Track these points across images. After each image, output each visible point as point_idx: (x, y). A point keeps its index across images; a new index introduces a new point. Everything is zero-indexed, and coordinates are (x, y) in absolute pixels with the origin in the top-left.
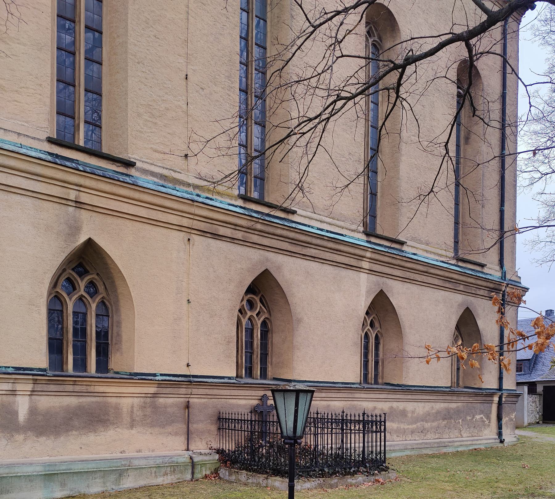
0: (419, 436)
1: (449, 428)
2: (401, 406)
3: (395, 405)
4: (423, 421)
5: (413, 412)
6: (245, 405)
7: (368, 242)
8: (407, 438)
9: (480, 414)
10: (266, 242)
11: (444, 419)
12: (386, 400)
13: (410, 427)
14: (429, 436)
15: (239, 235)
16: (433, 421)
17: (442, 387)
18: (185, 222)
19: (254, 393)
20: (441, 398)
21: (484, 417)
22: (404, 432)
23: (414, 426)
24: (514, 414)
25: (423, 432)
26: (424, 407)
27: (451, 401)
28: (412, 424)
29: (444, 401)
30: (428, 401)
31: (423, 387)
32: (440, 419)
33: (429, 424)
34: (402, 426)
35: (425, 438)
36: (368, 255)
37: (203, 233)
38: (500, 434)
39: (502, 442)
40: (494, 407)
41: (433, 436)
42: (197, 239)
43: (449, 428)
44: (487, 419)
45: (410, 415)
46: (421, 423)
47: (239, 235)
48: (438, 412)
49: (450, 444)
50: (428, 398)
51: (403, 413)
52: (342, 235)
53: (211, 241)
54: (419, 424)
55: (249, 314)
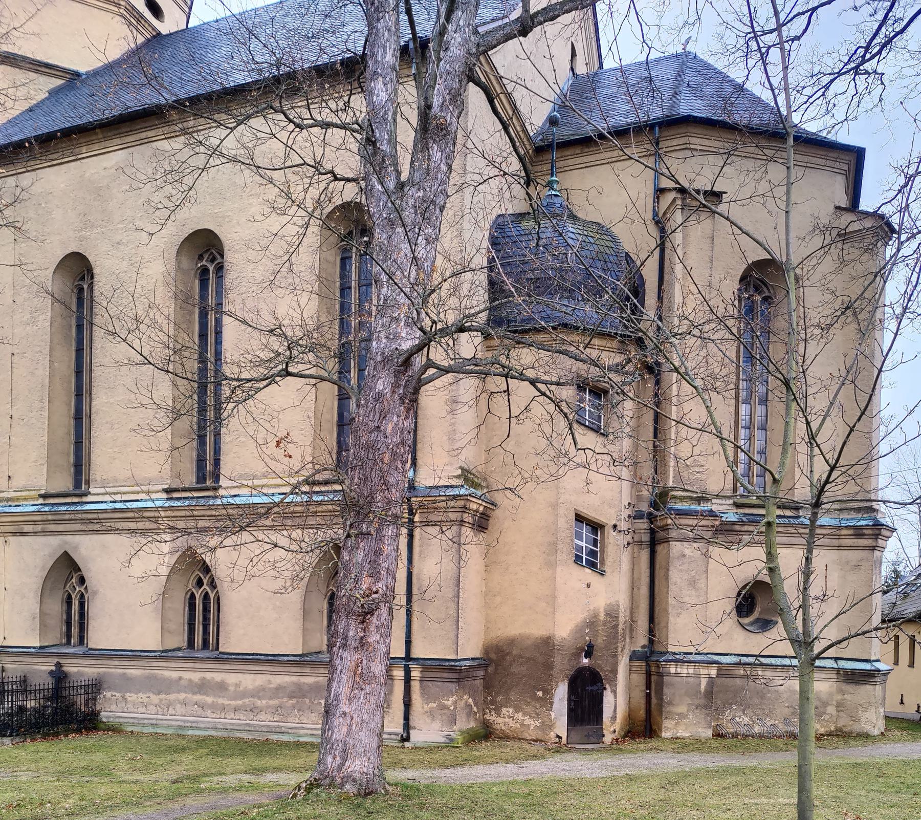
0: (244, 715)
1: (299, 710)
2: (218, 677)
3: (208, 675)
4: (253, 696)
5: (237, 685)
6: (45, 671)
7: (168, 499)
8: (227, 717)
10: (61, 528)
11: (291, 697)
12: (194, 670)
13: (233, 703)
14: (262, 716)
15: (39, 528)
16: (271, 699)
17: (288, 655)
20: (281, 669)
22: (223, 708)
23: (240, 702)
24: (451, 699)
25: (254, 710)
26: (254, 680)
27: (302, 675)
28: (235, 699)
29: (288, 673)
31: (252, 655)
32: (283, 697)
33: (264, 702)
34: (220, 701)
35: (255, 719)
36: (163, 514)
37: (14, 534)
38: (407, 726)
41: (270, 718)
42: (11, 539)
43: (299, 710)
45: (232, 688)
46: (251, 699)
47: (39, 528)
48: (279, 688)
49: (290, 731)
50: (257, 669)
51: (222, 687)
52: (137, 501)
53: (21, 538)
54: (246, 701)
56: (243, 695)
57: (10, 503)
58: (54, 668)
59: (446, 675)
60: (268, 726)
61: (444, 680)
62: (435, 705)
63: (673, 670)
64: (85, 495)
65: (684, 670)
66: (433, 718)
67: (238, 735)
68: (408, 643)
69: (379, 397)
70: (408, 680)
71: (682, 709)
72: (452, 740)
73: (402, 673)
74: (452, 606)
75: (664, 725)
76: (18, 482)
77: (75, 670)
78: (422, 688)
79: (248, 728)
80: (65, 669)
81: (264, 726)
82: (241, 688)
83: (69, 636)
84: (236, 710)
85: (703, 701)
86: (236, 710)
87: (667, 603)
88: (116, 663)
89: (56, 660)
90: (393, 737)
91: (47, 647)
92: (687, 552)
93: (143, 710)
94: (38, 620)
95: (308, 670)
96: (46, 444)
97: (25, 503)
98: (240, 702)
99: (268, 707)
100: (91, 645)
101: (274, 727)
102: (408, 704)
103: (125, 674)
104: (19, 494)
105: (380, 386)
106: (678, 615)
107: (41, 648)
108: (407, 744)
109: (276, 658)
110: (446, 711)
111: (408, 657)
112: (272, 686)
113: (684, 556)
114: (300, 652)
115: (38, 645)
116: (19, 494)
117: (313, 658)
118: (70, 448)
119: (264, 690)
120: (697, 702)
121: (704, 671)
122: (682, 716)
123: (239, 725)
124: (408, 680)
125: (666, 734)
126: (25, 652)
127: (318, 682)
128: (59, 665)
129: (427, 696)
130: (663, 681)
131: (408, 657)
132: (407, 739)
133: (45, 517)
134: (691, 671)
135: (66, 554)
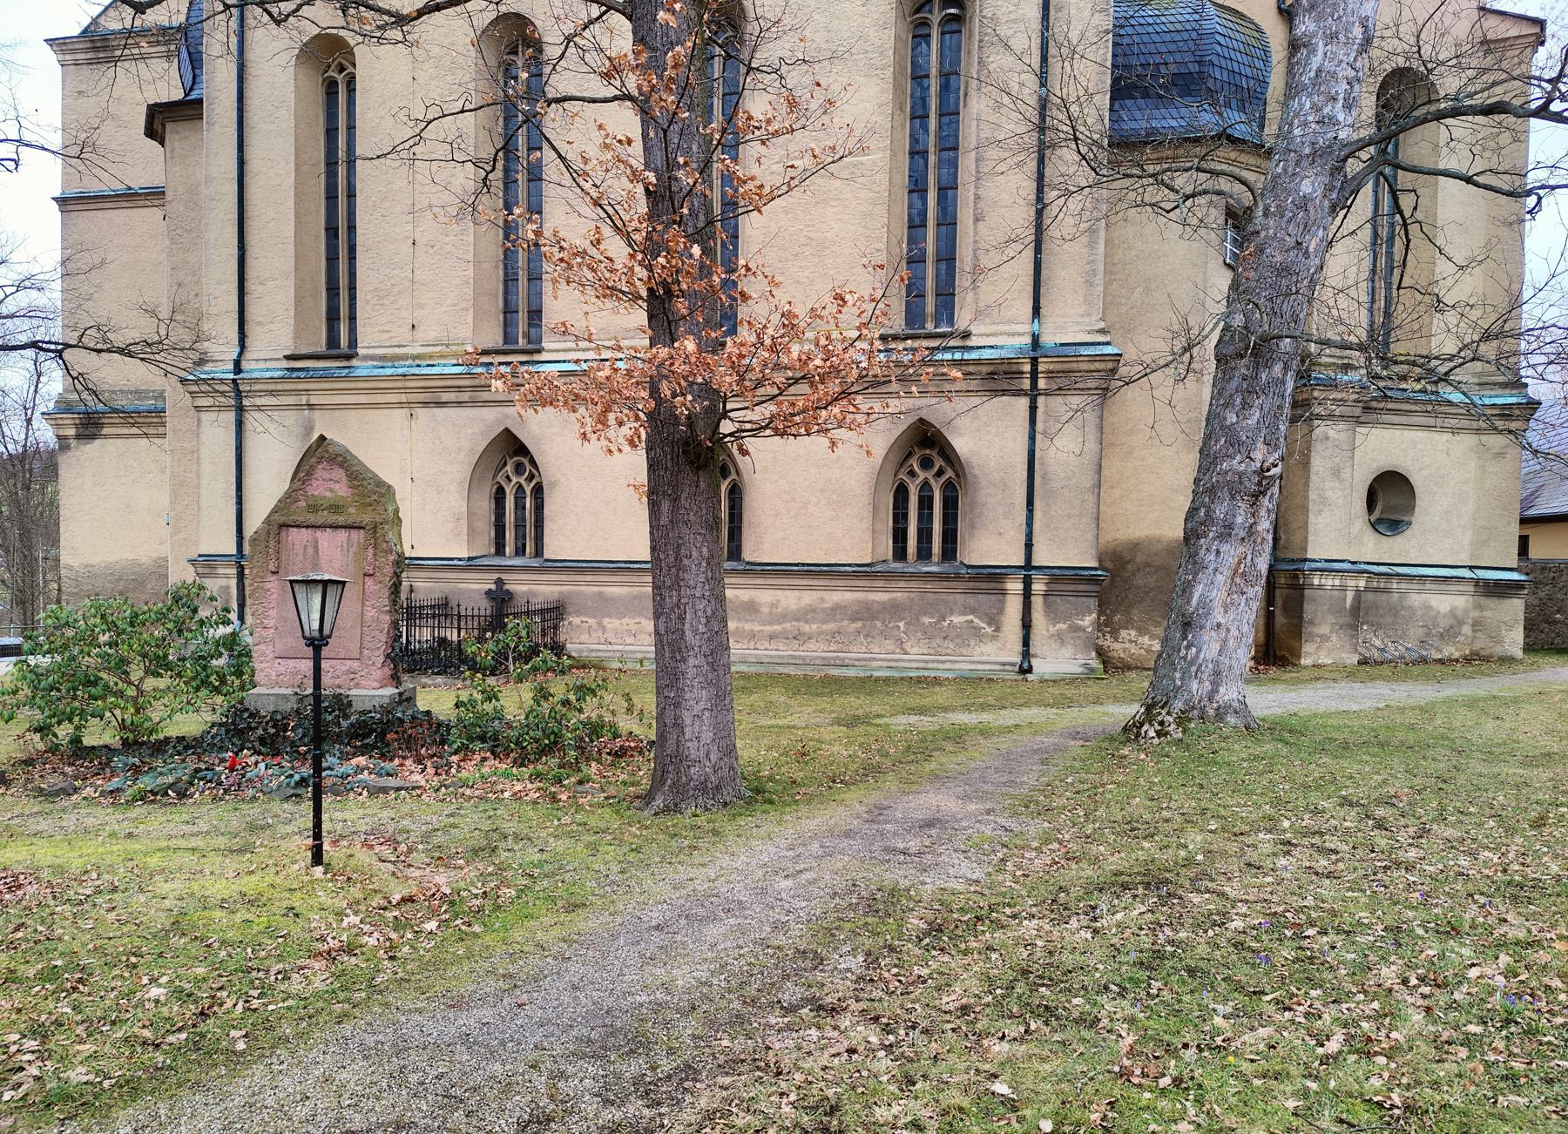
1: (867, 636)
4: (798, 620)
8: (758, 646)
9: (964, 614)
11: (854, 619)
13: (768, 628)
14: (812, 645)
15: (465, 396)
17: (850, 565)
18: (403, 398)
19: (486, 576)
20: (840, 583)
21: (976, 620)
22: (753, 636)
23: (778, 628)
26: (799, 599)
28: (770, 623)
29: (851, 589)
30: (810, 588)
31: (797, 565)
33: (814, 627)
34: (748, 626)
37: (425, 404)
38: (1026, 654)
39: (1025, 670)
40: (1014, 606)
43: (867, 636)
44: (989, 624)
45: (765, 610)
47: (465, 396)
48: (836, 609)
49: (857, 663)
54: (788, 625)
55: (514, 480)
56: (784, 617)
57: (418, 362)
58: (493, 587)
59: (1082, 587)
60: (824, 658)
61: (1077, 594)
62: (1065, 626)
63: (1316, 582)
64: (539, 351)
65: (1330, 581)
66: (1062, 643)
67: (781, 669)
68: (1029, 546)
69: (1304, 204)
70: (1027, 594)
71: (1324, 629)
72: (1092, 670)
73: (1020, 586)
74: (1092, 499)
75: (1304, 650)
76: (429, 332)
77: (524, 588)
78: (1047, 605)
79: (793, 661)
80: (507, 587)
81: (818, 658)
82: (780, 609)
83: (900, 536)
84: (771, 637)
85: (1348, 620)
86: (771, 637)
87: (1306, 498)
88: (589, 578)
89: (495, 576)
90: (1007, 667)
91: (476, 558)
92: (1331, 433)
93: (630, 640)
94: (464, 522)
95: (881, 584)
96: (471, 281)
97: (443, 362)
98: (778, 628)
99: (819, 634)
100: (546, 556)
101: (832, 658)
102: (1027, 625)
103: (601, 593)
104: (430, 349)
105: (1306, 187)
106: (1320, 512)
107: (470, 559)
108: (1030, 677)
109: (834, 569)
110: (1081, 634)
111: (1028, 565)
112: (826, 605)
113: (1328, 438)
114: (869, 561)
115: (466, 555)
116: (430, 349)
117: (879, 568)
118: (498, 287)
119: (814, 611)
120: (1342, 621)
121: (1351, 583)
122: (1325, 638)
123: (779, 657)
124: (1027, 594)
125: (1305, 661)
126: (447, 565)
127: (894, 599)
128: (499, 582)
129: (1052, 614)
130: (1303, 595)
131: (1028, 565)
132: (1030, 670)
133: (476, 382)
134: (1337, 582)
135: (507, 432)
